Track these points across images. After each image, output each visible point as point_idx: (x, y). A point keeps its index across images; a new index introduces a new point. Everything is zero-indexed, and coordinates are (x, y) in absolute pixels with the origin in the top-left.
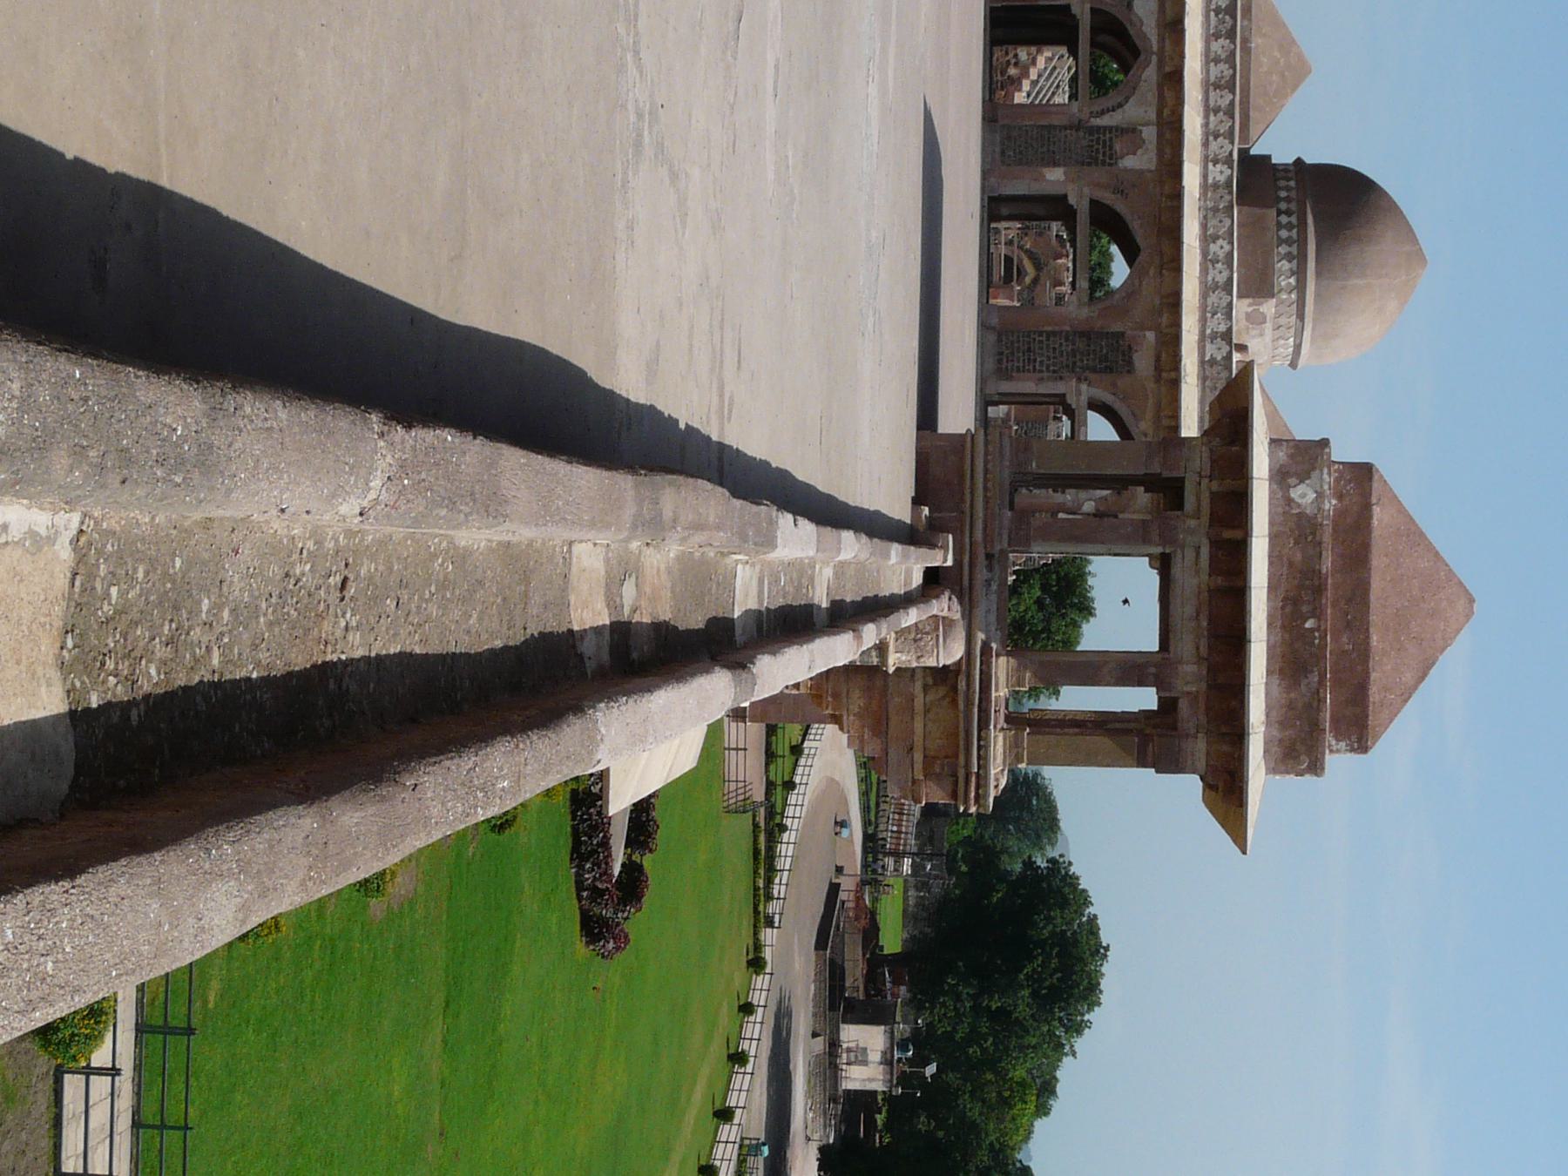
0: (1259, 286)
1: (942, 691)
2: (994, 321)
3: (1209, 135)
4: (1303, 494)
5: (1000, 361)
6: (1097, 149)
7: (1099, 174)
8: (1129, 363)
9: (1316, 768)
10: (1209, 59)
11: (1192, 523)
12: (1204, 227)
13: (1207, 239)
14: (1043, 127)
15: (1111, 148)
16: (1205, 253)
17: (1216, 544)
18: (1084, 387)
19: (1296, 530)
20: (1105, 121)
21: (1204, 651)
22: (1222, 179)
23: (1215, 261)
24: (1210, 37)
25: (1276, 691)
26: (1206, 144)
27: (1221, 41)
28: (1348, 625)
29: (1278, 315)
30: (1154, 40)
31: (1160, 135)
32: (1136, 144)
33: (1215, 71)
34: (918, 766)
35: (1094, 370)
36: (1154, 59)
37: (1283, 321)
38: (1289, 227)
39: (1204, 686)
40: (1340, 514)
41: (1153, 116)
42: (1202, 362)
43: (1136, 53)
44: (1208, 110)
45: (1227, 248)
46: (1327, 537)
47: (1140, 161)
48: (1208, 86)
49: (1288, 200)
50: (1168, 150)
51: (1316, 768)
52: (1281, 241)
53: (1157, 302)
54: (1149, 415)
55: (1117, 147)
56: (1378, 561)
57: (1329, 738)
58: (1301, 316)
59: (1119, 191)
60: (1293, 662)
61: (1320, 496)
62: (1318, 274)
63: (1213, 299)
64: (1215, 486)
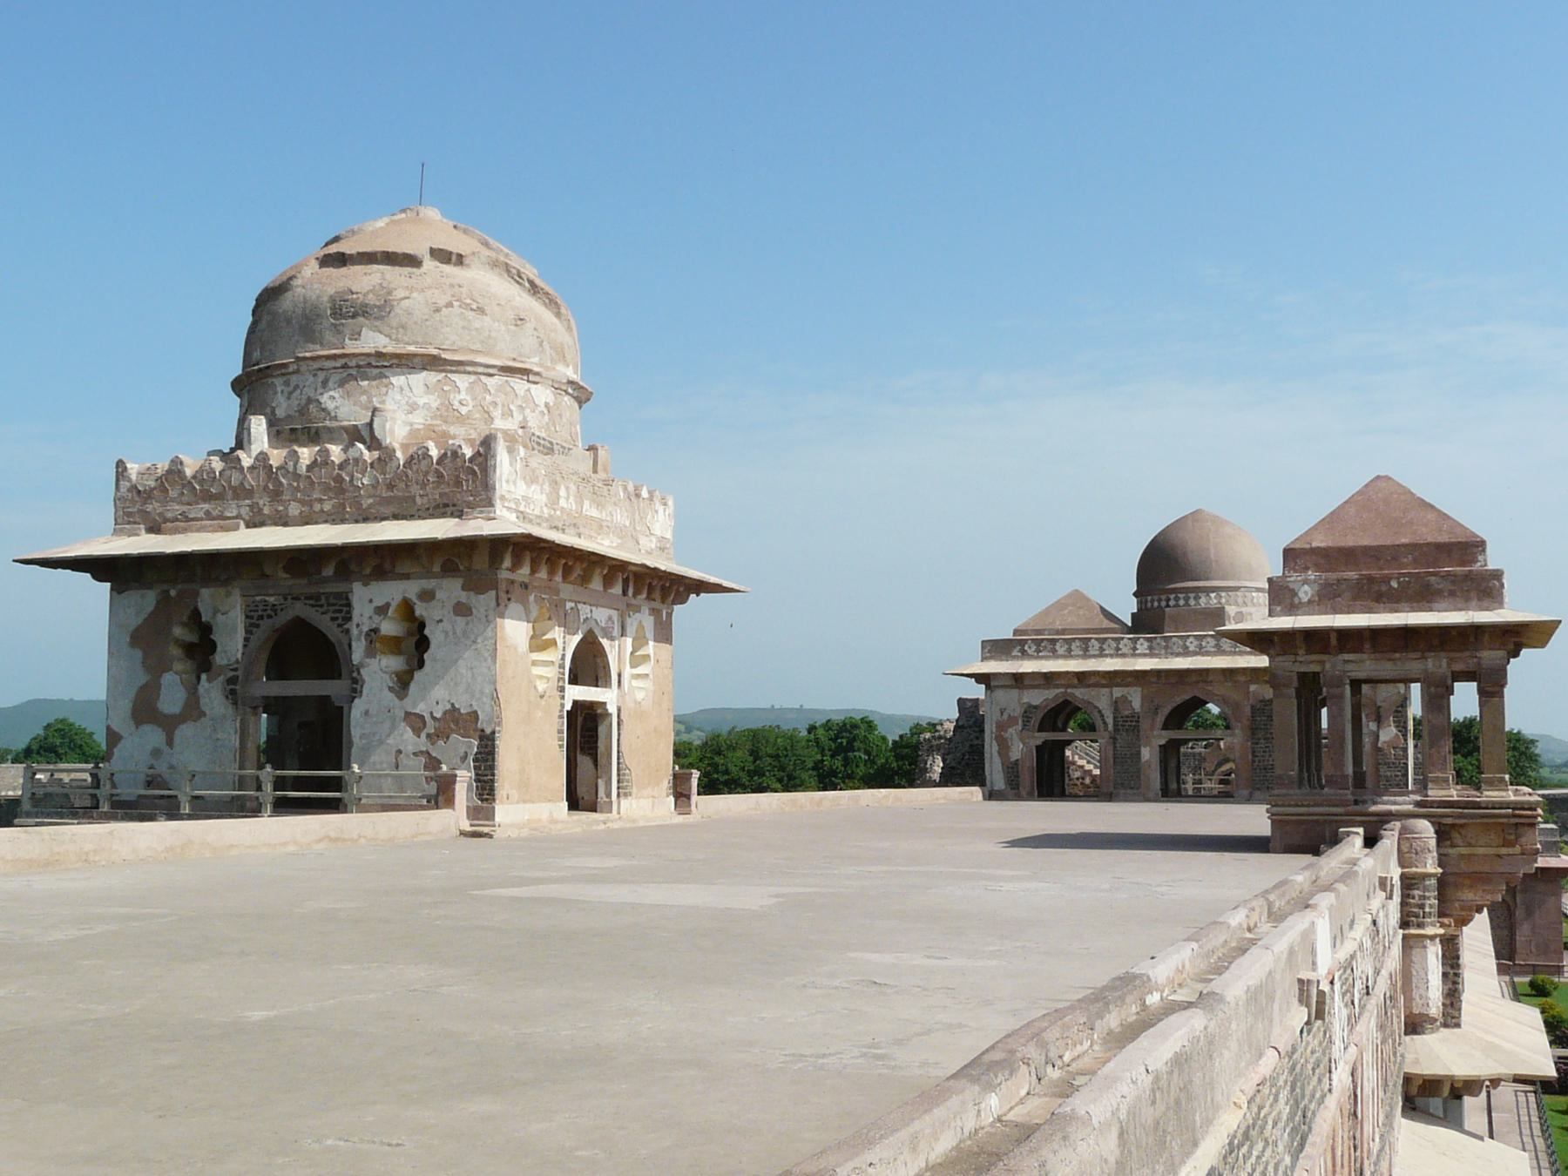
0: (1218, 615)
1: (1455, 835)
2: (1246, 792)
3: (1118, 653)
4: (1305, 593)
6: (1128, 726)
7: (1145, 725)
9: (1497, 575)
10: (1069, 655)
11: (1328, 666)
12: (1178, 655)
13: (1186, 653)
16: (1195, 654)
17: (1342, 649)
19: (1328, 598)
20: (1110, 721)
21: (1418, 655)
22: (1146, 644)
23: (1201, 647)
24: (1055, 655)
25: (1444, 605)
26: (1124, 656)
28: (1395, 559)
29: (1237, 604)
30: (1058, 691)
31: (1118, 685)
32: (1124, 699)
34: (1511, 851)
37: (1240, 600)
38: (1177, 599)
39: (1443, 654)
40: (1318, 568)
43: (1066, 703)
44: (1101, 654)
46: (1333, 576)
48: (1086, 655)
49: (1160, 600)
51: (1497, 575)
52: (1187, 604)
56: (1350, 542)
57: (1477, 567)
58: (1237, 589)
59: (1156, 711)
60: (1423, 596)
61: (1305, 582)
62: (1207, 579)
64: (1301, 652)
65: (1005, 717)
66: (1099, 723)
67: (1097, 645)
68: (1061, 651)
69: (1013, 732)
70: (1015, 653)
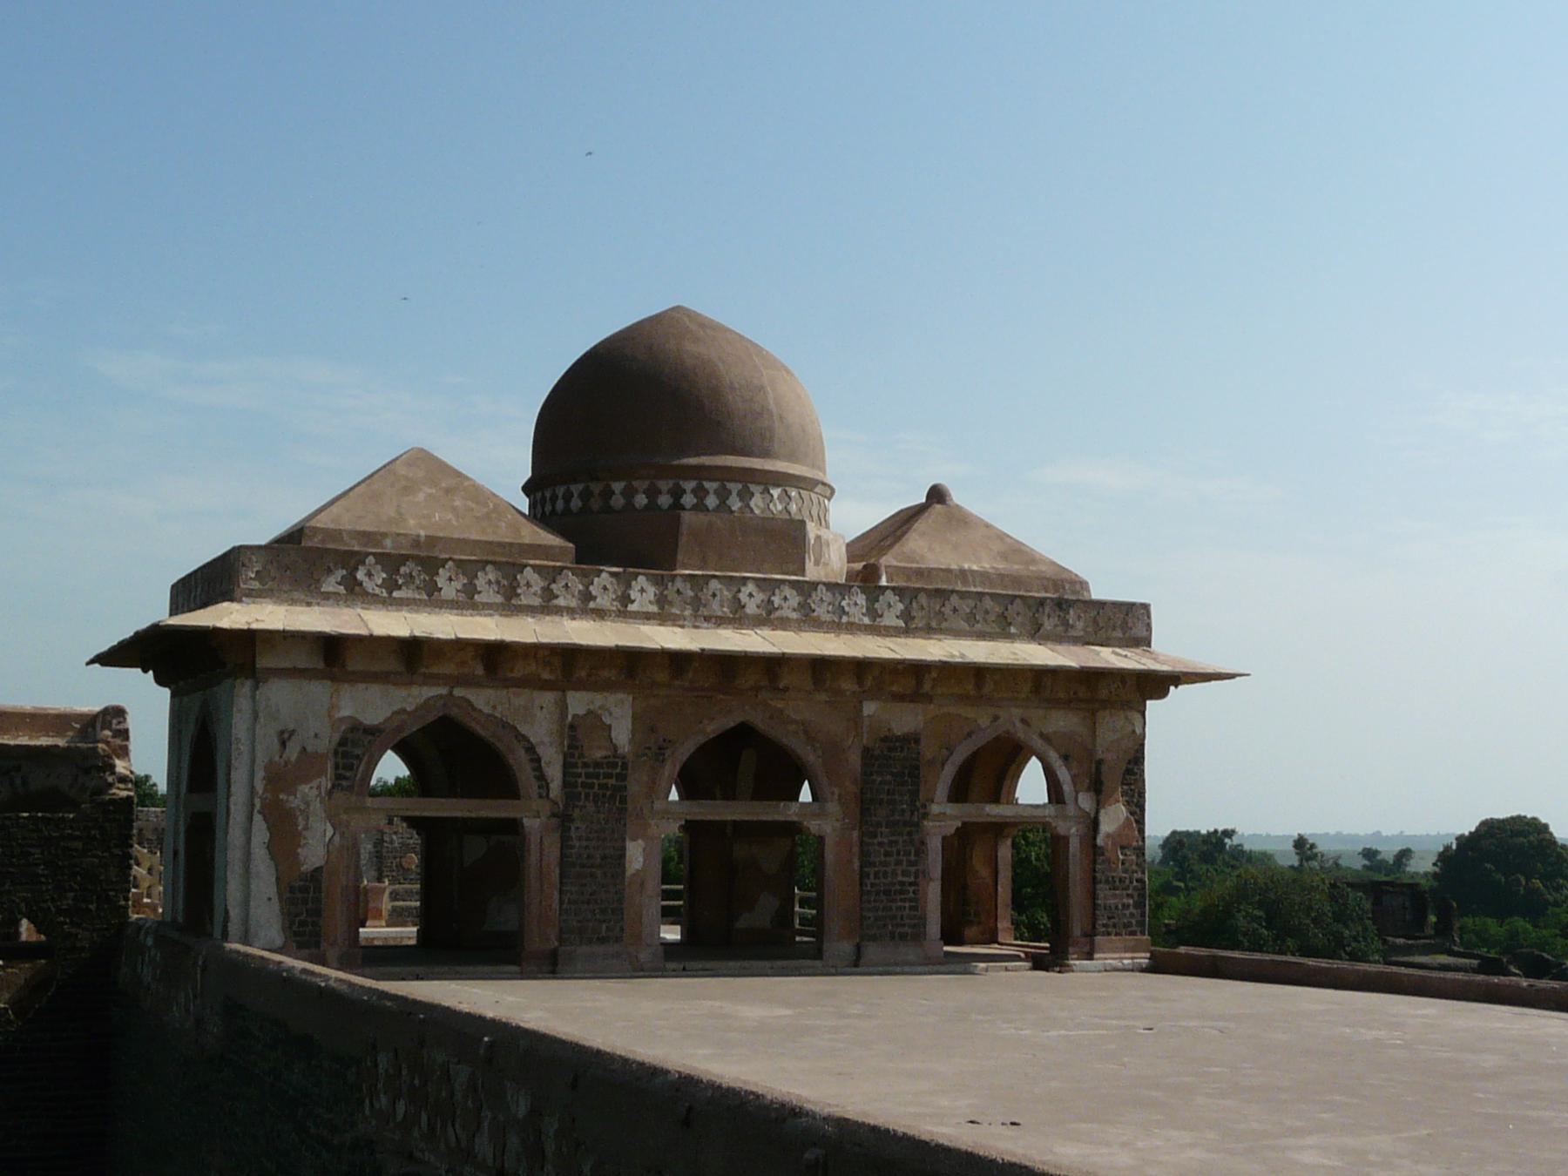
0: (788, 541)
2: (847, 947)
5: (903, 937)
8: (912, 739)
10: (468, 602)
12: (720, 621)
14: (562, 876)
15: (597, 765)
18: (935, 809)
20: (554, 773)
22: (651, 591)
23: (769, 607)
24: (432, 599)
27: (441, 581)
31: (581, 686)
32: (595, 723)
33: (488, 595)
35: (915, 794)
36: (458, 692)
38: (700, 492)
41: (548, 698)
42: (907, 632)
45: (751, 587)
47: (620, 719)
48: (510, 606)
49: (653, 493)
50: (606, 674)
52: (723, 506)
53: (823, 697)
54: (967, 712)
55: (598, 754)
62: (766, 454)
63: (822, 612)
65: (293, 752)
66: (525, 775)
67: (537, 582)
68: (449, 590)
69: (310, 794)
70: (331, 584)
